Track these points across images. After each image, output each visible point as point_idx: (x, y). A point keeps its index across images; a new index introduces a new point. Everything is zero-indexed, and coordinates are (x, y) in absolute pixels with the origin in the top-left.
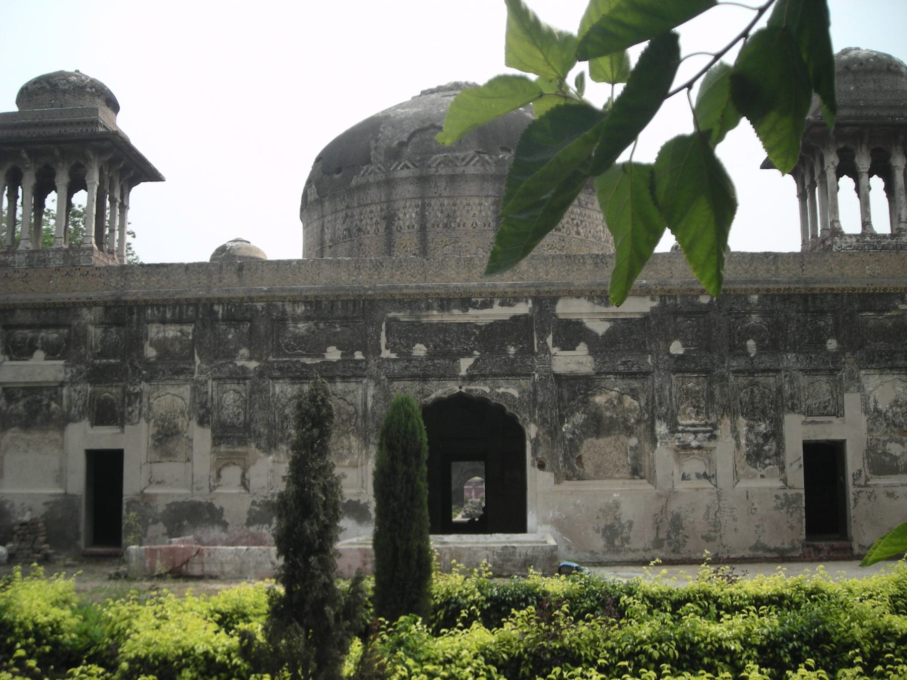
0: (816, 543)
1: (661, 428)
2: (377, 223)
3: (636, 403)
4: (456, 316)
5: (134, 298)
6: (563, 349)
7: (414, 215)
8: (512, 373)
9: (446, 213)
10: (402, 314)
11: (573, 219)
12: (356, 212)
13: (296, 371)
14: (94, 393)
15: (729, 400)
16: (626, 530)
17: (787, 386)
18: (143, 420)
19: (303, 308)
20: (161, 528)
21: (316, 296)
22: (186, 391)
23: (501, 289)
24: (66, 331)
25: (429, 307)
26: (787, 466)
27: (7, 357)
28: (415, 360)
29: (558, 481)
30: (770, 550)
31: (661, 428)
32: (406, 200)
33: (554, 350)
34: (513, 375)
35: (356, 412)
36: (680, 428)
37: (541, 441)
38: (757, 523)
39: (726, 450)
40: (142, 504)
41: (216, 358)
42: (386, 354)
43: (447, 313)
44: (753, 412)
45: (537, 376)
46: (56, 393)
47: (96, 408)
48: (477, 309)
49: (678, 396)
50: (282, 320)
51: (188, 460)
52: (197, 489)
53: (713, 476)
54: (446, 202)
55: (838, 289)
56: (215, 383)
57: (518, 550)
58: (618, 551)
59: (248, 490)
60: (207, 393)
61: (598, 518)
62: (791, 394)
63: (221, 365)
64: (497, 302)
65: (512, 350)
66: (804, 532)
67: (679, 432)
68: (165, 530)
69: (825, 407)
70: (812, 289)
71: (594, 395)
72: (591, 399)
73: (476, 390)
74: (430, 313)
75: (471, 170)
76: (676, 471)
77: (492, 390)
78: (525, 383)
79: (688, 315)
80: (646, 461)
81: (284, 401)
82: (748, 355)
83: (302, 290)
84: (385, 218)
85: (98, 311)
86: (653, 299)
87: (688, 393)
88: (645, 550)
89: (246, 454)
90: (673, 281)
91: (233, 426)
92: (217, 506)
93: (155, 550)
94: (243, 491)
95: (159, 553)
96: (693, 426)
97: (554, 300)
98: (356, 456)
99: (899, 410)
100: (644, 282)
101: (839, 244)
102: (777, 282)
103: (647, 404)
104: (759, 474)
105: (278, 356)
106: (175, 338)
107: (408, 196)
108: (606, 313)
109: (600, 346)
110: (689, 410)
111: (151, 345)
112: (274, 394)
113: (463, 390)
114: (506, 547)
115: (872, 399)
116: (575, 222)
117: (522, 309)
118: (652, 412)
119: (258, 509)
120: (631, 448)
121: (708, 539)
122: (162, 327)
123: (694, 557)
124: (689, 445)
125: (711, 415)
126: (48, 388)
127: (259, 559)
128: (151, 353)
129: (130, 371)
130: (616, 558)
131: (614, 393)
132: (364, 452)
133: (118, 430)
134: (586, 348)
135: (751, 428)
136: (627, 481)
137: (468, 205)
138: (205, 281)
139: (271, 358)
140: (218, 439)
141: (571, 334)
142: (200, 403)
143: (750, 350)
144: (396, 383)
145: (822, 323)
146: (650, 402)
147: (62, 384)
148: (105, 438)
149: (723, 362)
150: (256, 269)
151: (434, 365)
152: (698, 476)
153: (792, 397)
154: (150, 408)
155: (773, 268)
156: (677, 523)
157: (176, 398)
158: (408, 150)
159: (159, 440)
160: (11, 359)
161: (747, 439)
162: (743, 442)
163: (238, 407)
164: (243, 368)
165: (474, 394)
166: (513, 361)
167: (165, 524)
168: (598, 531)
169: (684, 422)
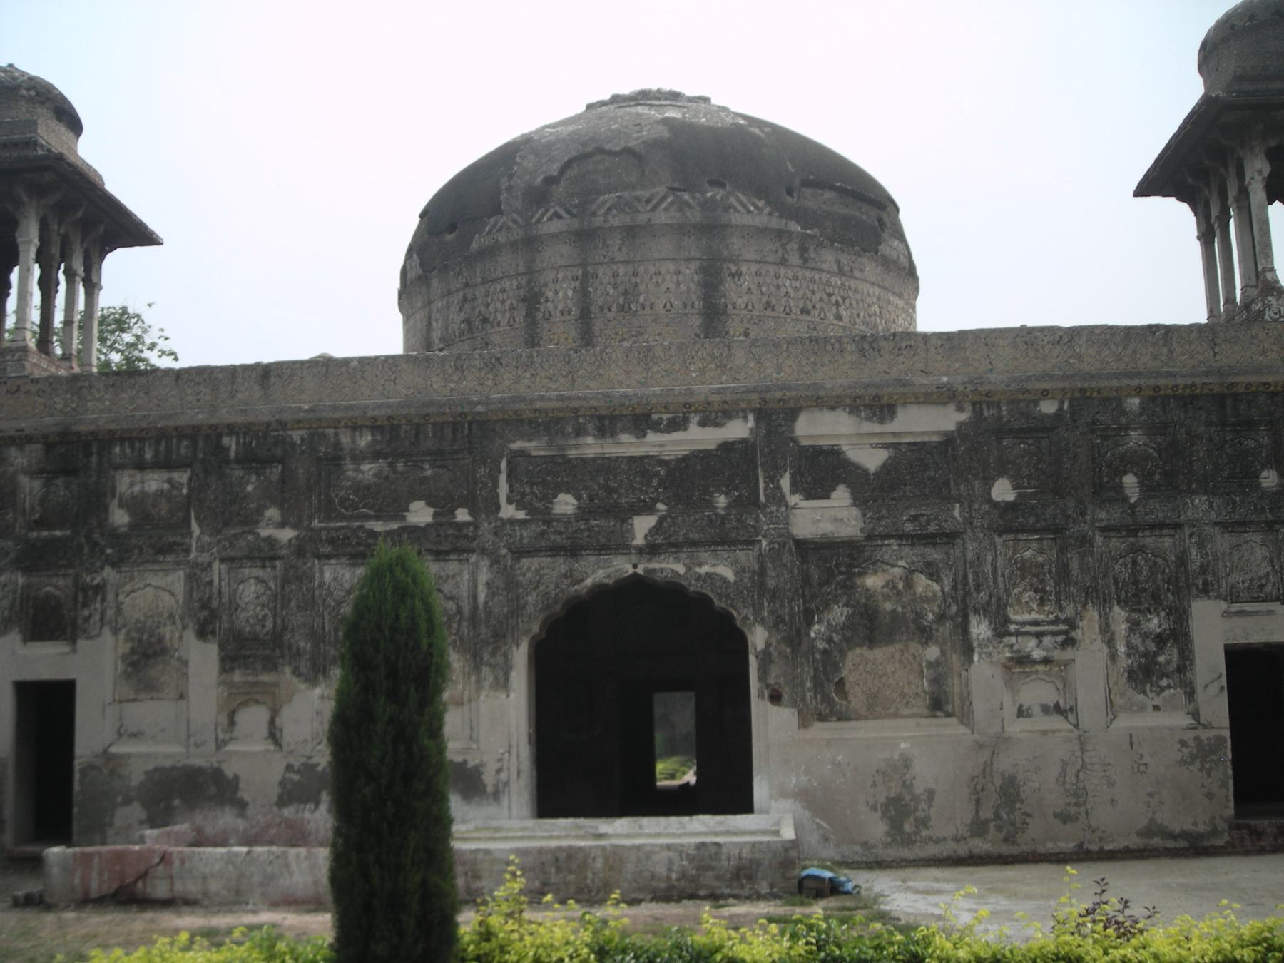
0: (1252, 822)
1: (980, 629)
2: (512, 308)
3: (936, 587)
4: (626, 445)
5: (92, 428)
6: (807, 499)
7: (570, 293)
8: (721, 538)
9: (622, 288)
10: (533, 444)
11: (830, 295)
12: (479, 292)
13: (359, 544)
14: (27, 587)
15: (1095, 578)
16: (923, 805)
17: (1194, 552)
18: (106, 631)
19: (369, 438)
20: (136, 811)
21: (390, 418)
22: (177, 580)
23: (702, 398)
25: (580, 431)
26: (1199, 689)
28: (558, 521)
29: (804, 723)
30: (1173, 836)
31: (980, 629)
32: (557, 269)
33: (794, 499)
34: (723, 543)
35: (459, 611)
36: (1012, 628)
37: (775, 654)
38: (1150, 789)
39: (1093, 663)
40: (106, 772)
41: (226, 524)
42: (508, 511)
43: (609, 440)
44: (1137, 598)
45: (764, 543)
47: (31, 611)
48: (662, 432)
49: (1007, 572)
50: (335, 460)
51: (182, 697)
52: (197, 745)
53: (1071, 709)
54: (622, 270)
55: (1276, 384)
56: (223, 566)
57: (725, 850)
58: (908, 842)
59: (281, 746)
60: (210, 583)
61: (874, 785)
62: (1201, 566)
63: (234, 536)
64: (695, 419)
65: (722, 501)
66: (1231, 804)
67: (1011, 634)
68: (143, 815)
69: (1261, 587)
70: (1232, 384)
71: (863, 574)
72: (858, 581)
73: (662, 570)
74: (581, 440)
75: (661, 218)
76: (1007, 701)
77: (689, 568)
78: (745, 557)
79: (1021, 434)
80: (954, 686)
81: (338, 594)
82: (1125, 499)
83: (366, 407)
84: (524, 300)
85: (36, 450)
86: (960, 409)
87: (1025, 568)
88: (956, 839)
89: (276, 685)
90: (992, 377)
91: (255, 638)
92: (229, 772)
93: (90, 855)
94: (272, 748)
95: (96, 860)
96: (1035, 623)
97: (792, 415)
98: (460, 687)
100: (945, 379)
101: (1275, 308)
102: (1171, 375)
103: (954, 588)
104: (1150, 704)
105: (328, 519)
106: (160, 493)
107: (560, 263)
108: (880, 435)
109: (873, 491)
110: (1025, 598)
111: (121, 506)
112: (322, 584)
113: (640, 570)
114: (703, 844)
116: (833, 299)
117: (738, 430)
118: (964, 600)
119: (296, 777)
120: (930, 664)
121: (1064, 818)
122: (138, 477)
123: (1041, 849)
124: (1028, 656)
125: (1064, 604)
127: (269, 869)
128: (120, 518)
129: (86, 549)
130: (907, 853)
131: (896, 571)
132: (473, 678)
133: (66, 649)
134: (848, 495)
135: (1134, 626)
136: (924, 721)
137: (658, 273)
138: (208, 398)
139: (316, 524)
140: (229, 661)
141: (822, 471)
142: (200, 600)
143: (1128, 492)
144: (525, 562)
145: (1252, 444)
146: (960, 583)
148: (45, 660)
149: (1083, 514)
150: (292, 375)
151: (590, 529)
152: (1045, 710)
153: (1204, 569)
154: (119, 611)
155: (1165, 351)
156: (1010, 792)
157: (161, 593)
158: (561, 189)
159: (134, 664)
161: (1129, 645)
162: (1121, 649)
163: (263, 606)
164: (271, 541)
165: (659, 577)
166: (724, 519)
167: (144, 805)
168: (874, 808)
169: (1018, 618)
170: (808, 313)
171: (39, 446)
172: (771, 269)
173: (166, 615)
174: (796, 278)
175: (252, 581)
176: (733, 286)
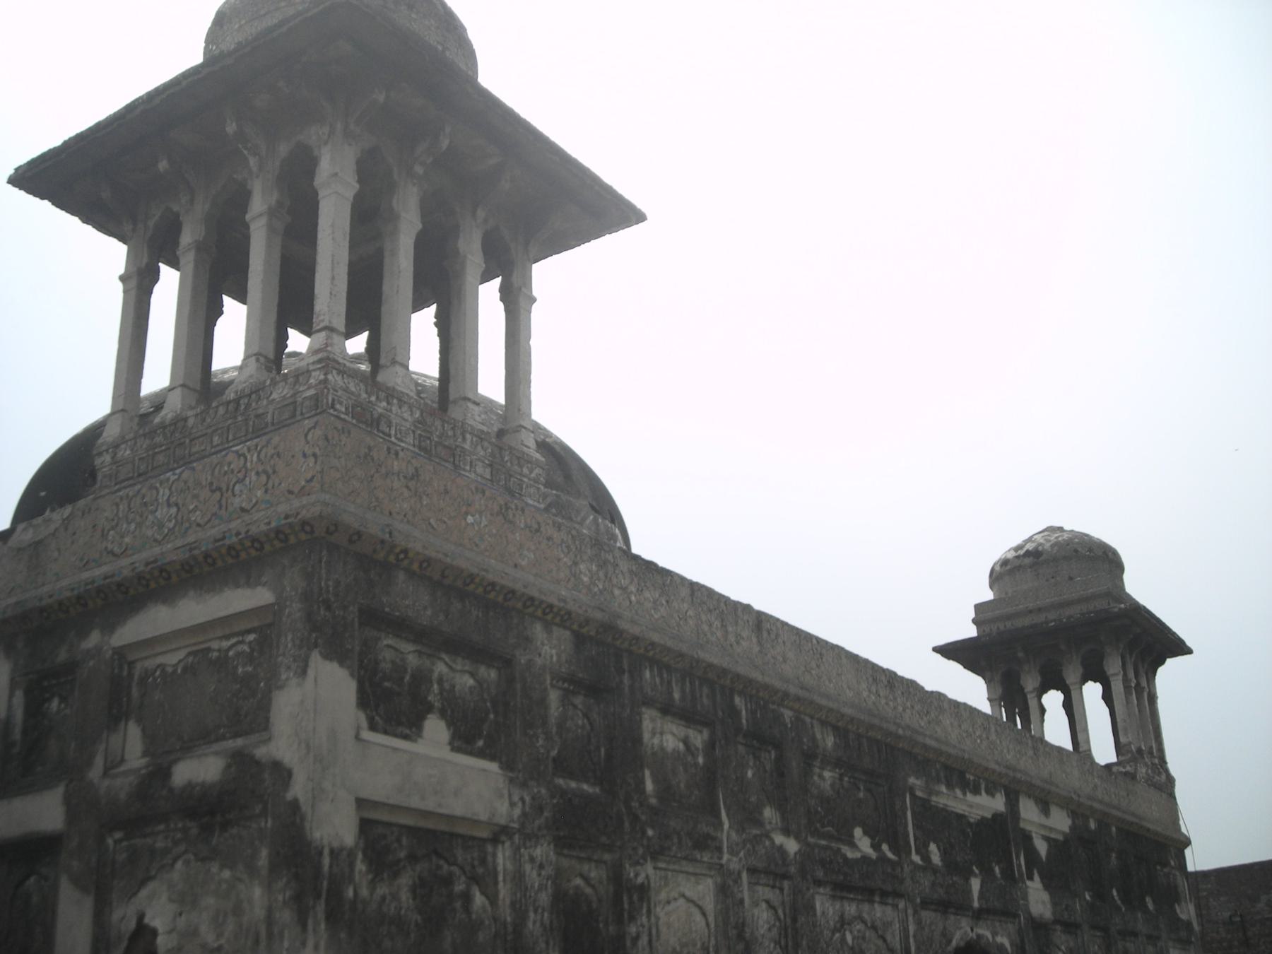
5: (636, 630)
24: (493, 674)
27: (362, 718)
46: (483, 861)
60: (742, 901)
63: (755, 836)
126: (468, 841)
129: (627, 824)
147: (500, 834)
160: (373, 727)
171: (568, 633)
173: (699, 945)
175: (764, 905)
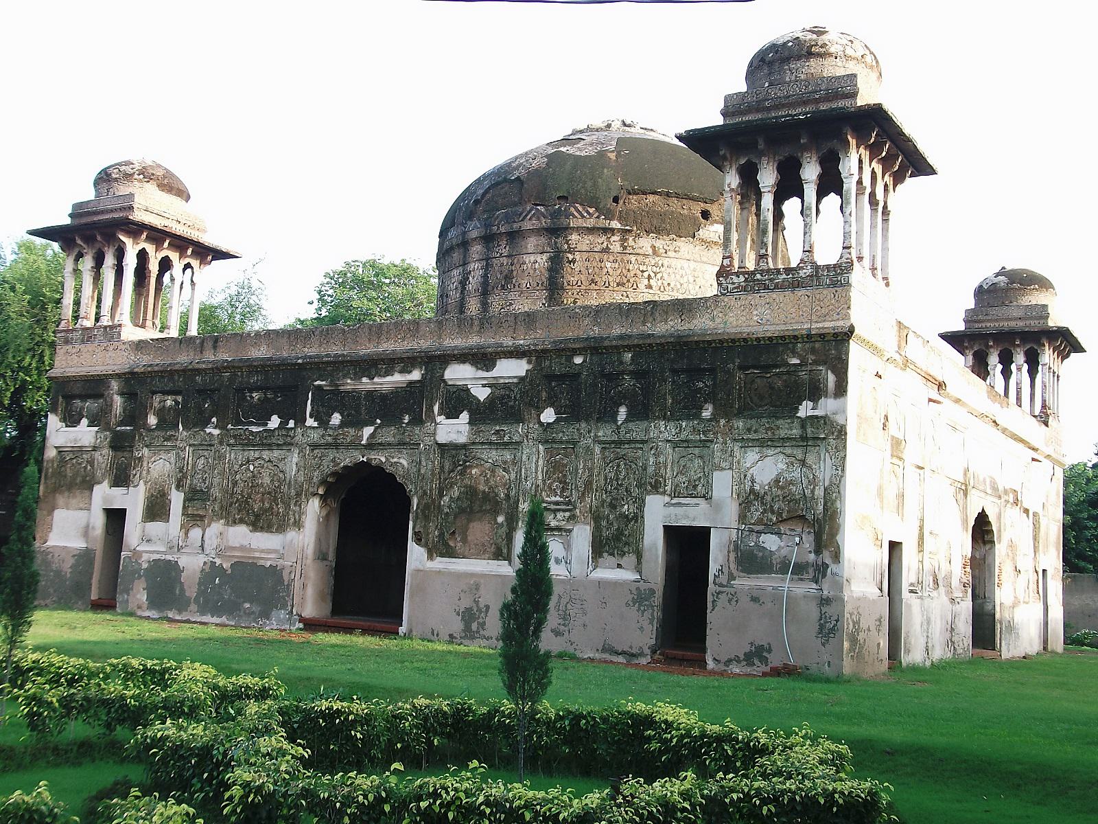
4: (366, 384)
6: (448, 418)
33: (440, 419)
42: (310, 422)
56: (191, 448)
69: (695, 487)
82: (615, 421)
86: (529, 362)
96: (557, 503)
99: (779, 492)
100: (522, 342)
106: (170, 408)
113: (365, 459)
115: (749, 477)
116: (646, 274)
117: (416, 375)
141: (457, 401)
145: (701, 385)
149: (589, 432)
170: (623, 285)
172: (597, 256)
174: (615, 261)
176: (569, 269)
